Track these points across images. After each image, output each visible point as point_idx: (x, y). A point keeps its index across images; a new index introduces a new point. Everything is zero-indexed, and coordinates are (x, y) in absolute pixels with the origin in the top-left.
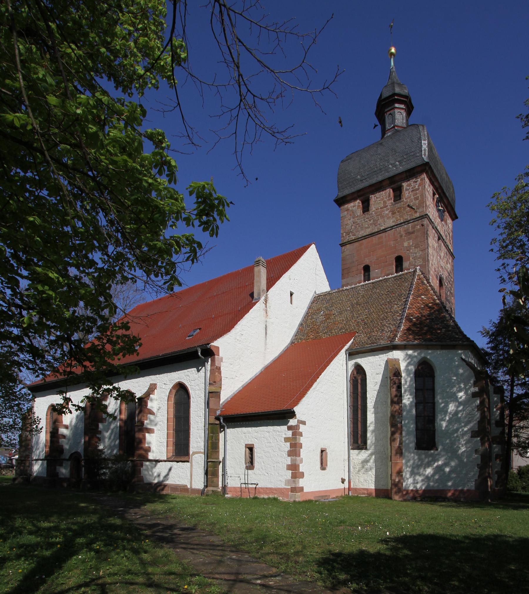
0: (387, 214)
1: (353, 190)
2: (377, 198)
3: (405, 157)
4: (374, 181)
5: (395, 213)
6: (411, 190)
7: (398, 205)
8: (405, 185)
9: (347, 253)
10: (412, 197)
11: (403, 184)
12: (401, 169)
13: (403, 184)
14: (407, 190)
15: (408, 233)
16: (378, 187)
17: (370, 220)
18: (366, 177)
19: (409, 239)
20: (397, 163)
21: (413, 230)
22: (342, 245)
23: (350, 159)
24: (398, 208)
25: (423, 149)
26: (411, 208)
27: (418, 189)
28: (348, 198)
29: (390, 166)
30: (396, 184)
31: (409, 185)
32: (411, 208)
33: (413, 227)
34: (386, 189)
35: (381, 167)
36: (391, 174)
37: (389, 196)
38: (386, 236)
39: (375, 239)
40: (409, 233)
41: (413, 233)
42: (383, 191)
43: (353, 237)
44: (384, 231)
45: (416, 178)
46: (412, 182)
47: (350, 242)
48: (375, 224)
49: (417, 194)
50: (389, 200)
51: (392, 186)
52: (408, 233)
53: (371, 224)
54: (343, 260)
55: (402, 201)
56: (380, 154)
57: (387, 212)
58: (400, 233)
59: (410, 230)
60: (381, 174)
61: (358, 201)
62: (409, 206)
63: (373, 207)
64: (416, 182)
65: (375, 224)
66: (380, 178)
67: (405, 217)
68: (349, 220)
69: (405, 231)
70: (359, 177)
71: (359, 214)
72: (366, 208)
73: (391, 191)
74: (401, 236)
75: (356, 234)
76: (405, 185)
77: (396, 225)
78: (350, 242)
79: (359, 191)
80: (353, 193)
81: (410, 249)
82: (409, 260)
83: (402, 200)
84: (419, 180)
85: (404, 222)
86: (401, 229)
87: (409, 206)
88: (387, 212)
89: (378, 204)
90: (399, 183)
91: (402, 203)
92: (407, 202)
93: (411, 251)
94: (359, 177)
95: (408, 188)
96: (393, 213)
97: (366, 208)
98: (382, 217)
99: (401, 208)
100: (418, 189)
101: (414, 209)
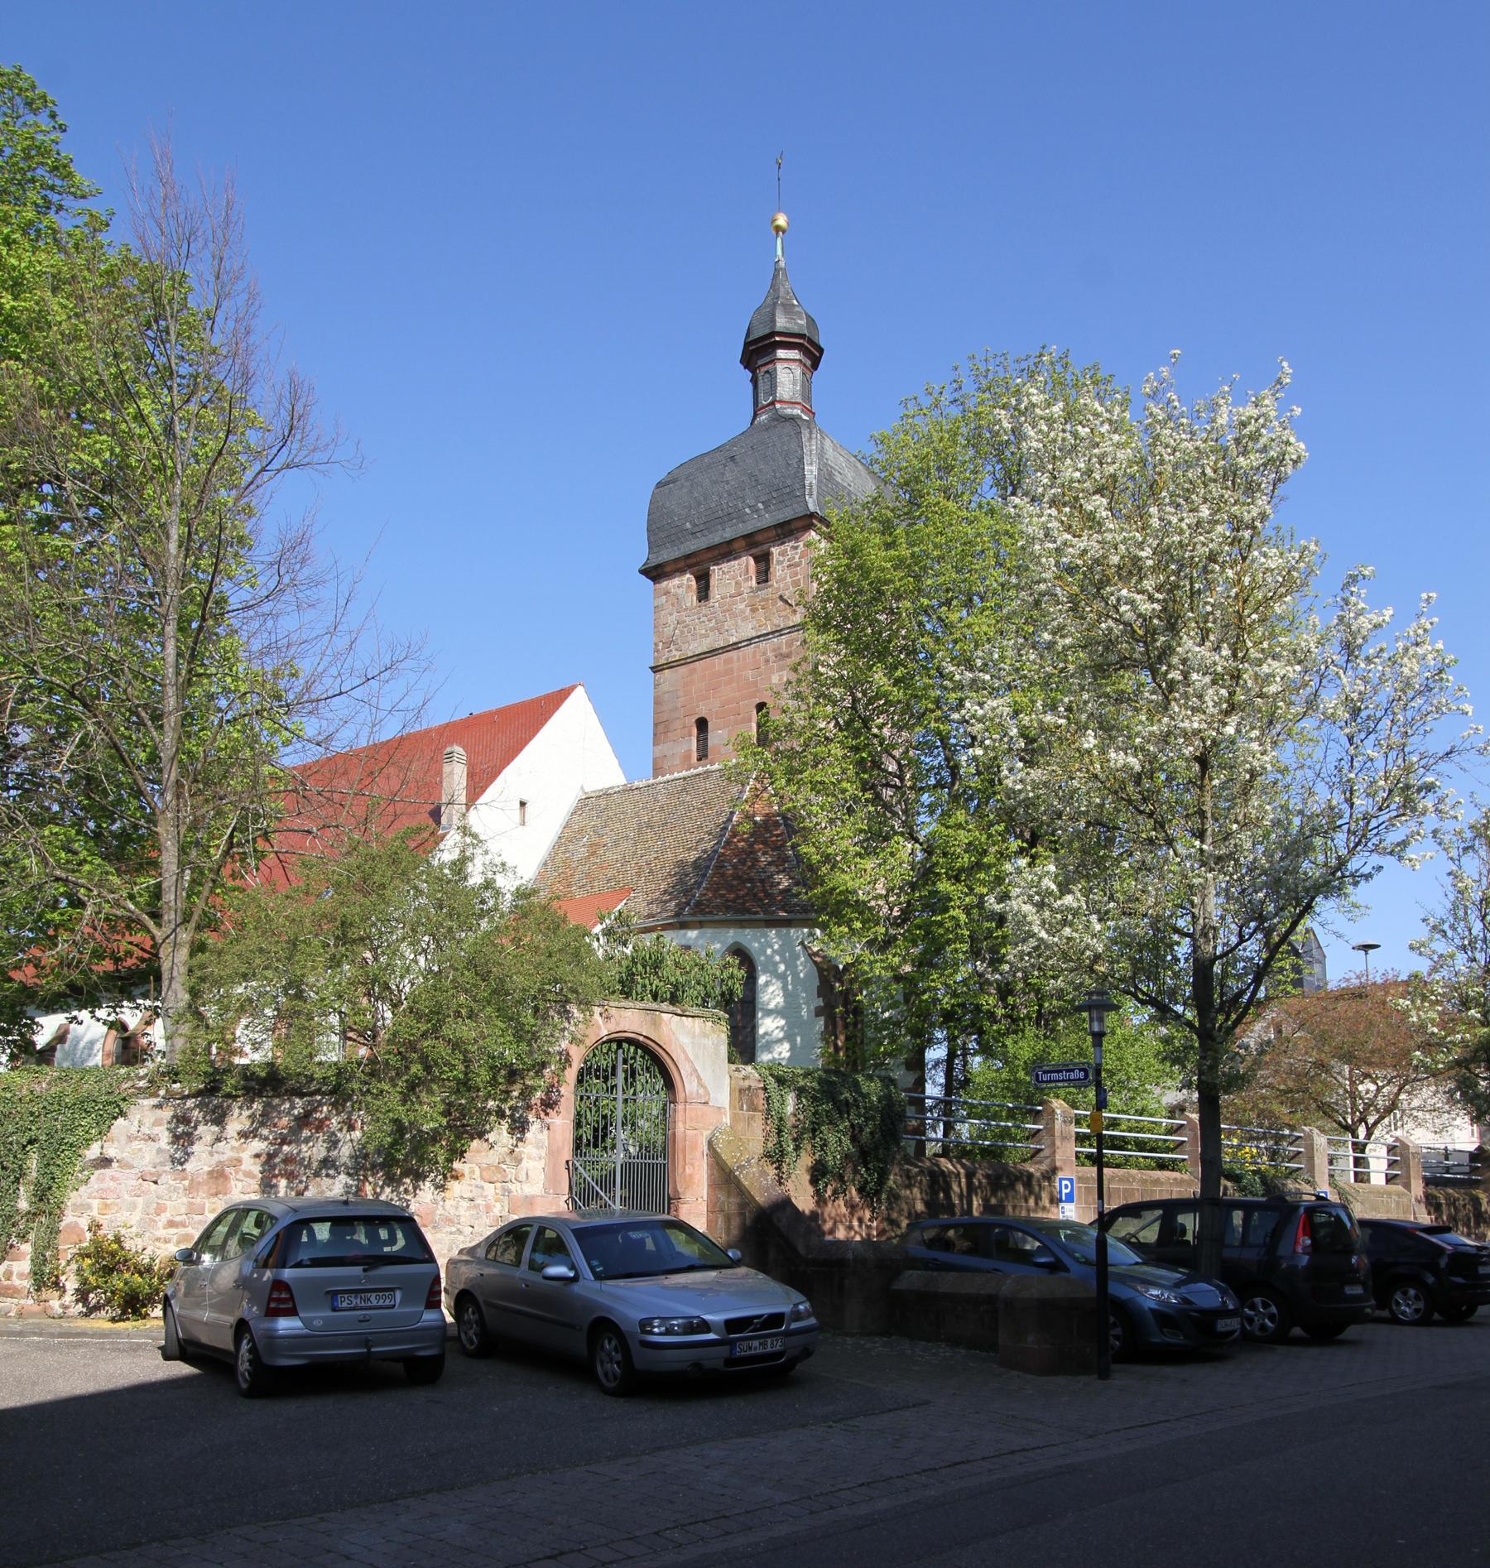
0: (743, 612)
1: (676, 553)
2: (724, 573)
3: (775, 495)
4: (716, 538)
5: (757, 609)
6: (786, 564)
8: (775, 550)
9: (665, 687)
10: (789, 580)
11: (773, 549)
12: (768, 519)
13: (773, 549)
14: (780, 563)
16: (725, 552)
17: (709, 620)
18: (702, 527)
20: (760, 506)
22: (656, 669)
23: (673, 481)
24: (763, 600)
25: (807, 482)
26: (786, 602)
27: (798, 565)
28: (668, 569)
29: (747, 510)
30: (760, 549)
31: (783, 554)
32: (786, 602)
33: (789, 644)
34: (740, 557)
35: (731, 510)
36: (748, 528)
37: (747, 572)
38: (738, 658)
39: (718, 661)
42: (735, 559)
43: (677, 655)
44: (735, 646)
45: (797, 539)
46: (788, 546)
47: (670, 665)
48: (718, 629)
49: (796, 574)
50: (746, 580)
51: (753, 551)
53: (712, 629)
54: (657, 702)
56: (728, 483)
57: (742, 606)
58: (764, 654)
59: (784, 650)
60: (730, 523)
61: (688, 576)
62: (781, 598)
63: (716, 592)
64: (796, 548)
65: (718, 629)
66: (728, 534)
67: (776, 621)
68: (671, 614)
69: (774, 650)
70: (688, 525)
71: (689, 605)
72: (704, 593)
73: (751, 561)
74: (767, 661)
75: (684, 647)
76: (775, 550)
77: (758, 637)
78: (670, 665)
79: (688, 557)
80: (676, 560)
84: (801, 544)
85: (772, 633)
86: (766, 646)
87: (781, 598)
88: (742, 606)
89: (726, 586)
90: (765, 547)
92: (778, 589)
94: (688, 525)
95: (781, 558)
96: (754, 610)
97: (704, 593)
98: (734, 616)
99: (767, 600)
100: (798, 565)
101: (791, 605)
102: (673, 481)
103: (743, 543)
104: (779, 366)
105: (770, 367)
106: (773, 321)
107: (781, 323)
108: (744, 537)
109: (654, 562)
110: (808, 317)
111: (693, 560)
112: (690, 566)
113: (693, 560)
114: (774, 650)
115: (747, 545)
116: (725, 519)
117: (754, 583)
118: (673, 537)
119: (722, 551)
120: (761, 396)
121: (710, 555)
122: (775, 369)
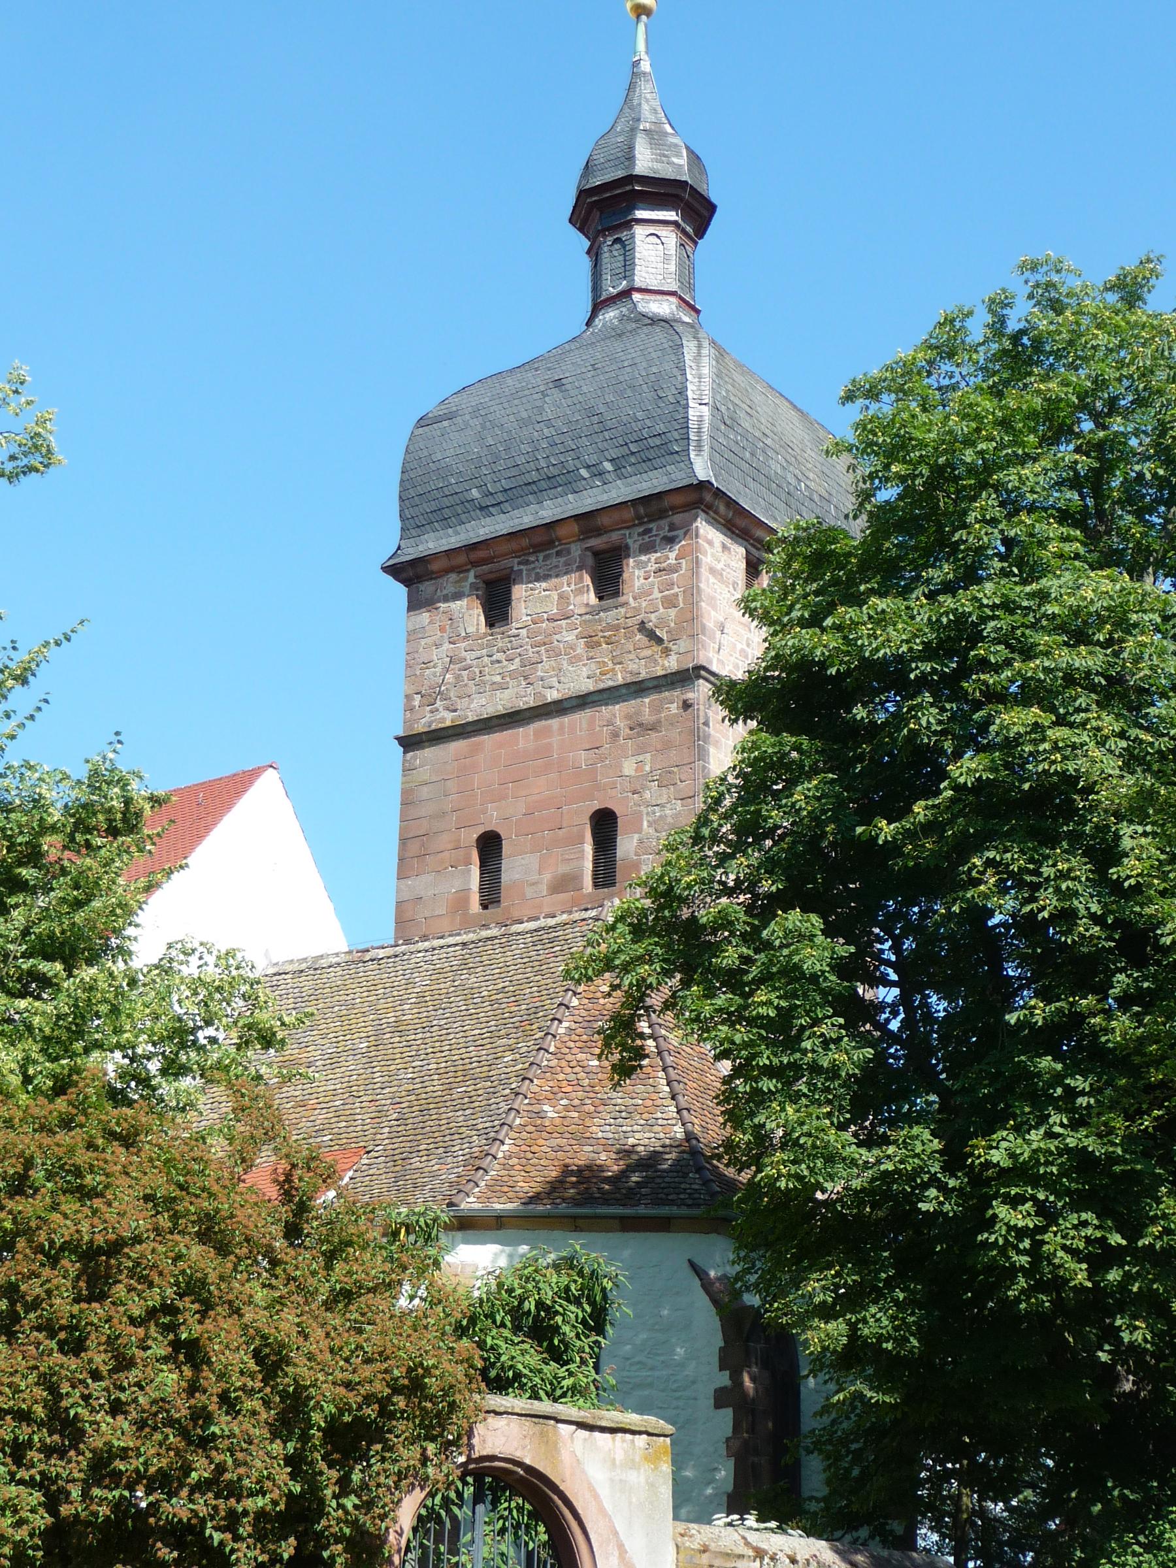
4: (527, 517)
7: (609, 617)
15: (641, 728)
19: (641, 750)
21: (653, 718)
40: (641, 725)
41: (653, 728)
52: (641, 728)
55: (622, 605)
57: (570, 637)
59: (647, 716)
67: (632, 667)
74: (615, 735)
81: (644, 787)
82: (639, 831)
83: (622, 599)
91: (622, 610)
93: (647, 795)
96: (592, 643)
99: (616, 628)
102: (450, 416)
103: (575, 528)
104: (640, 231)
105: (624, 235)
106: (630, 158)
107: (645, 162)
108: (577, 518)
109: (412, 552)
110: (690, 152)
111: (481, 554)
112: (475, 564)
113: (481, 554)
114: (628, 717)
115: (582, 532)
116: (543, 485)
117: (592, 598)
118: (447, 513)
119: (537, 539)
120: (607, 278)
121: (514, 545)
122: (633, 237)
